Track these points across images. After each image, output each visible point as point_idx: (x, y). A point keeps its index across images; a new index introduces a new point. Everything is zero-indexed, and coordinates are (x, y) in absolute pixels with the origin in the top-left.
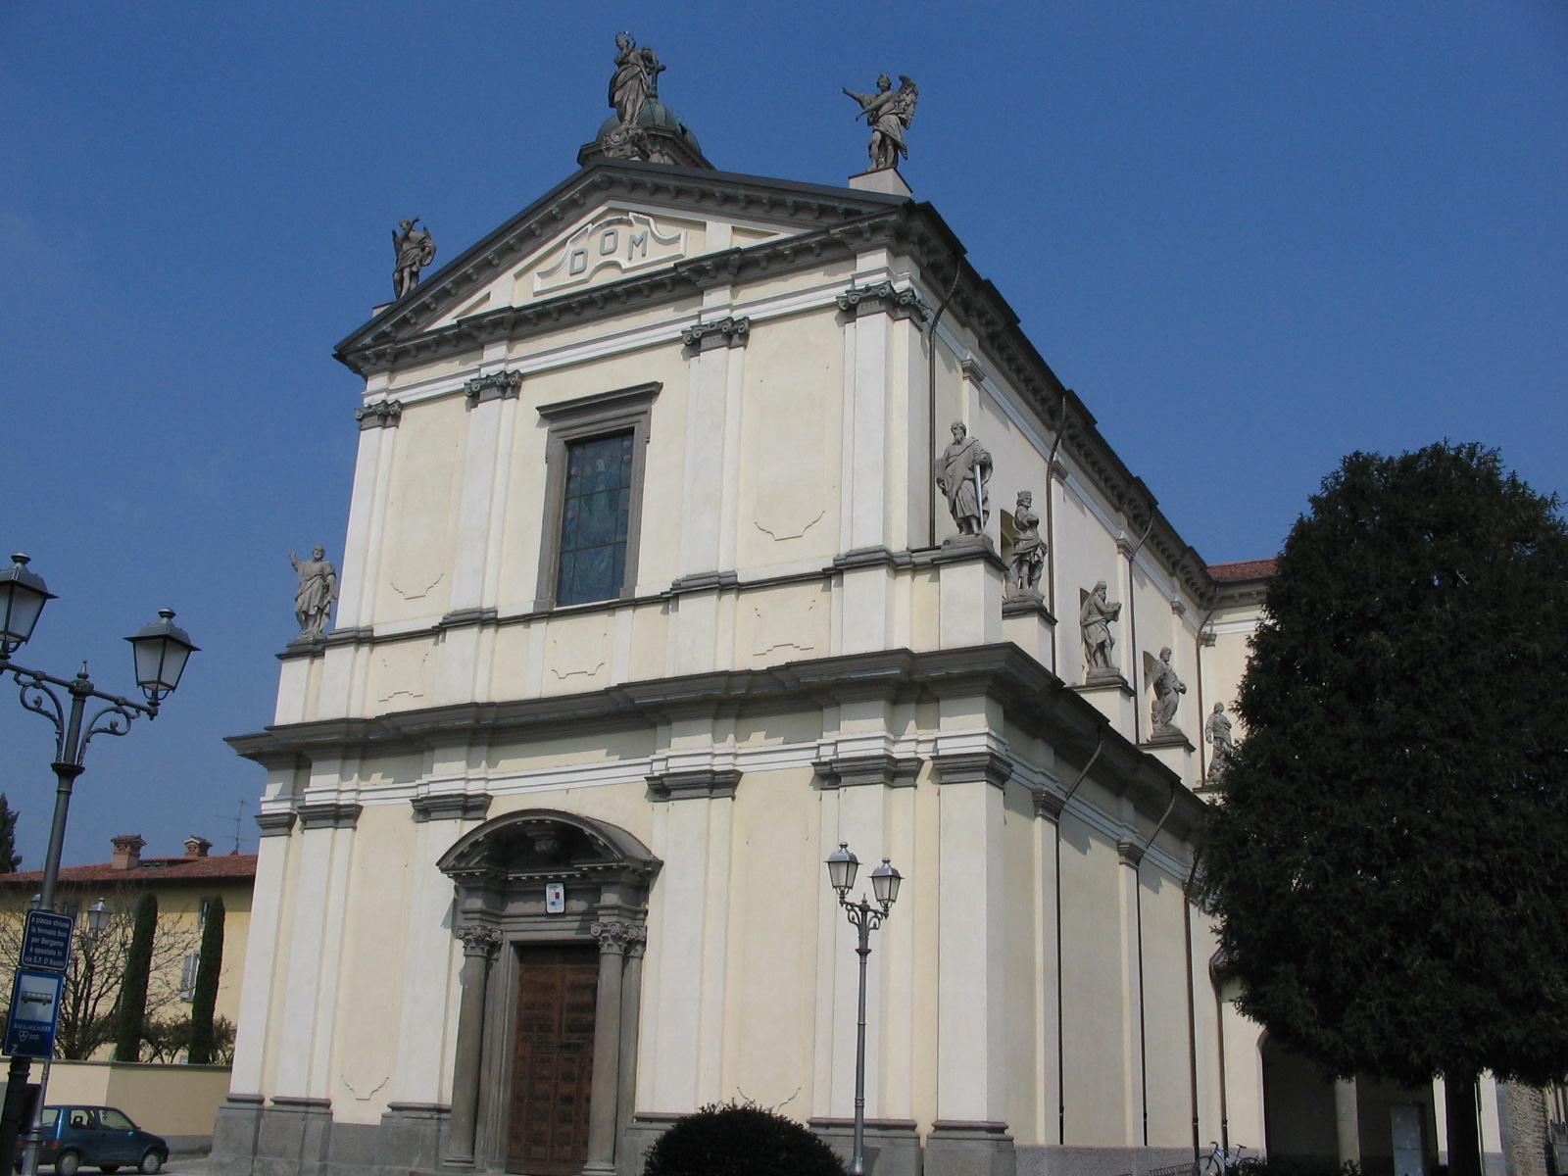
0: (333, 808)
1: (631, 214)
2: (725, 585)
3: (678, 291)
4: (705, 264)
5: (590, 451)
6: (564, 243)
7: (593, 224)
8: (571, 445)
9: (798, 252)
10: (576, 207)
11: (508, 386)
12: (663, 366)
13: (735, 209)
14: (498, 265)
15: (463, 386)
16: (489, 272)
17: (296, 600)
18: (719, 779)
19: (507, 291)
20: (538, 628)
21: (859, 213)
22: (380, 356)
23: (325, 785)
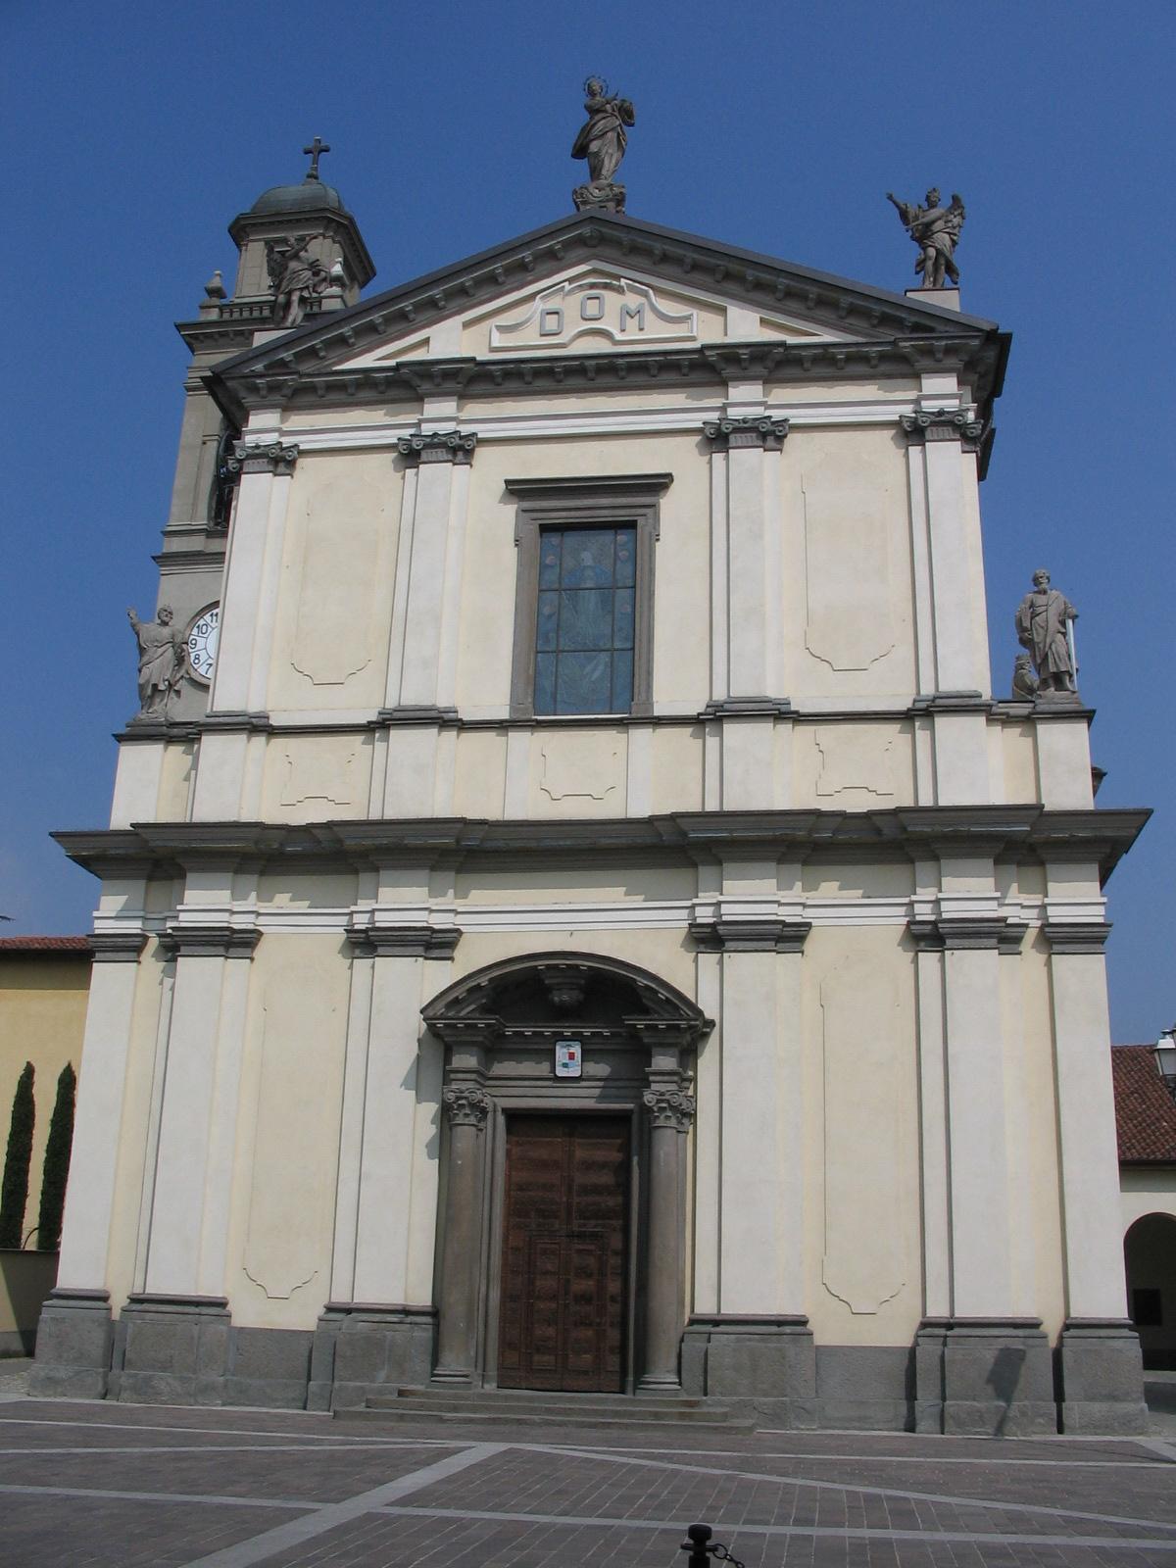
0: (227, 933)
1: (622, 280)
2: (781, 714)
3: (694, 377)
4: (741, 351)
5: (571, 540)
6: (532, 297)
7: (570, 284)
8: (545, 529)
9: (850, 359)
10: (553, 260)
11: (460, 449)
12: (680, 458)
13: (768, 299)
14: (444, 307)
15: (396, 441)
16: (431, 314)
17: (140, 671)
18: (438, 938)
19: (449, 339)
20: (519, 739)
21: (932, 330)
22: (273, 388)
23: (205, 902)
